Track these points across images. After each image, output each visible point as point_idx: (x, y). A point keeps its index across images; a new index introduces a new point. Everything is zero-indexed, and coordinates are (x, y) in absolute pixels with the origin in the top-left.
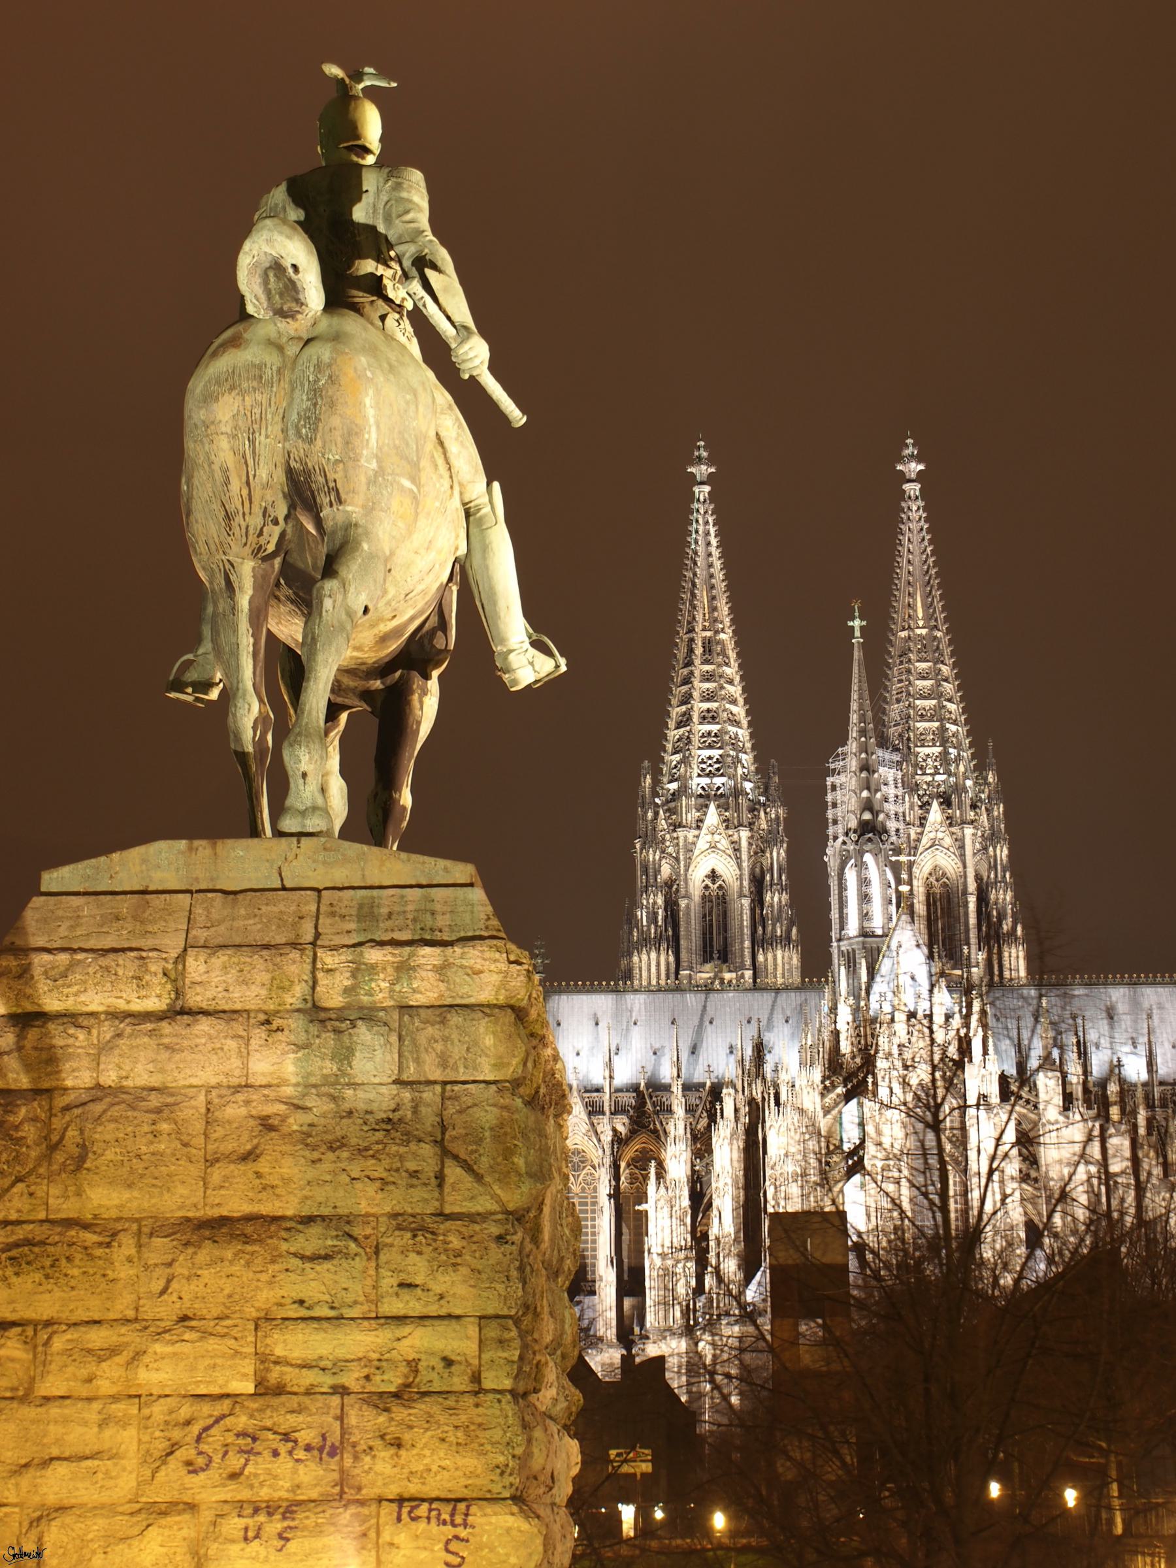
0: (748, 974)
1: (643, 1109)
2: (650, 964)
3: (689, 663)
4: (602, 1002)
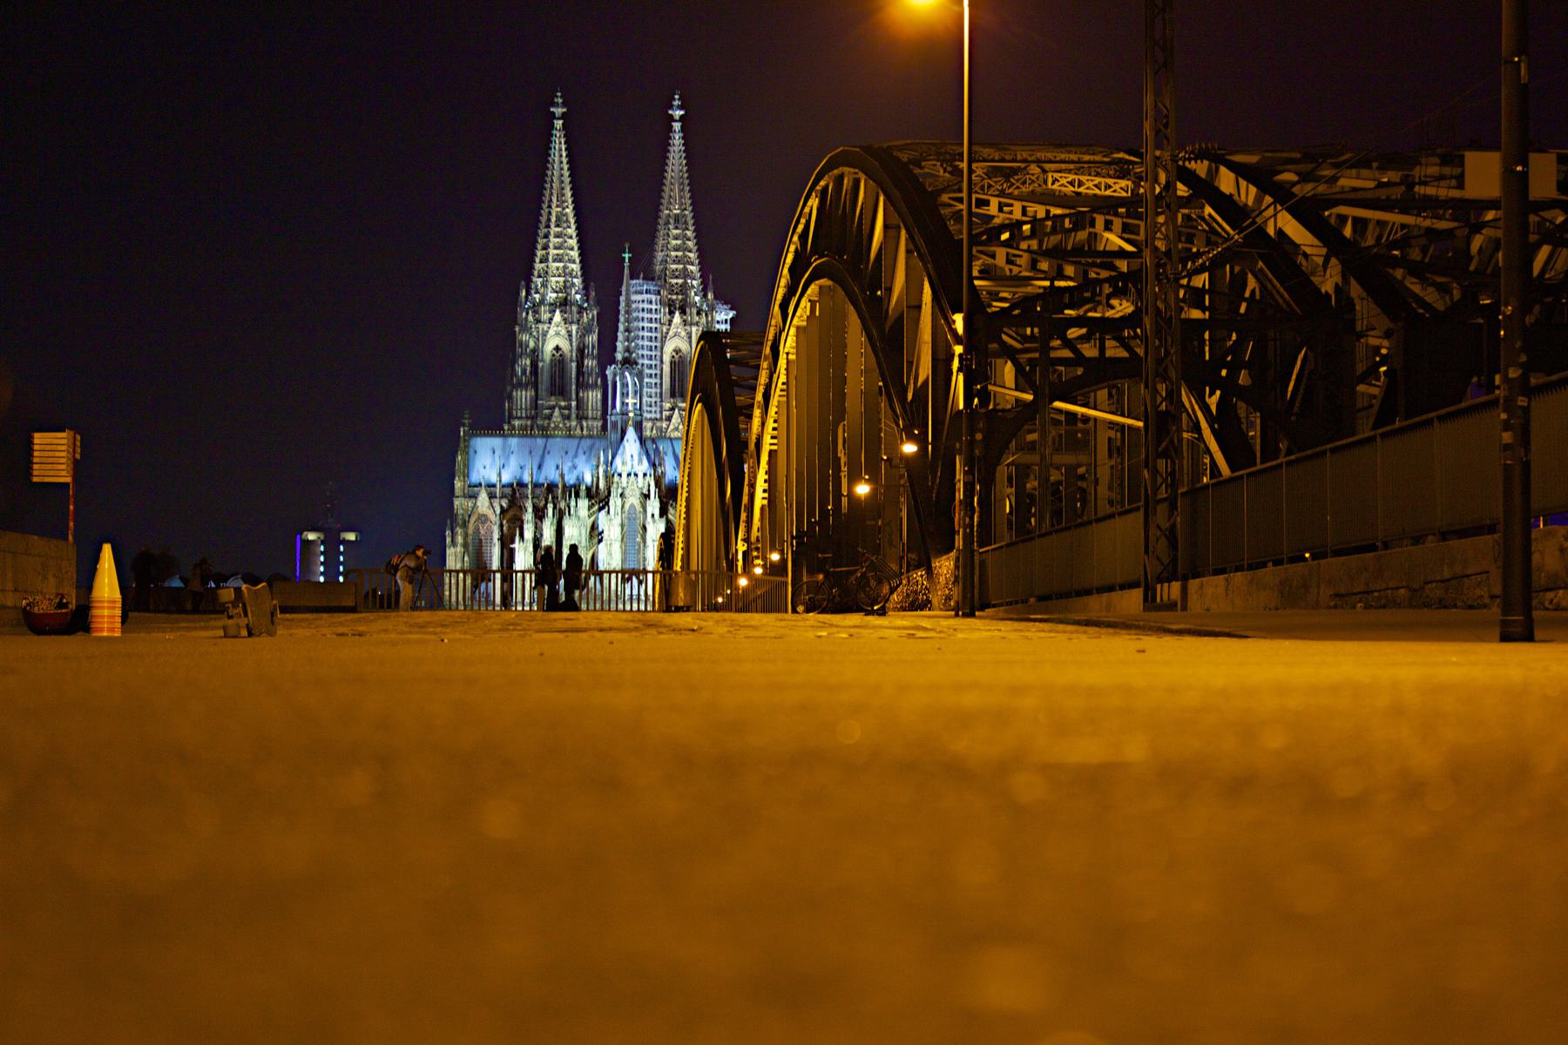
0: (574, 404)
1: (513, 495)
2: (523, 397)
3: (548, 226)
4: (496, 442)
